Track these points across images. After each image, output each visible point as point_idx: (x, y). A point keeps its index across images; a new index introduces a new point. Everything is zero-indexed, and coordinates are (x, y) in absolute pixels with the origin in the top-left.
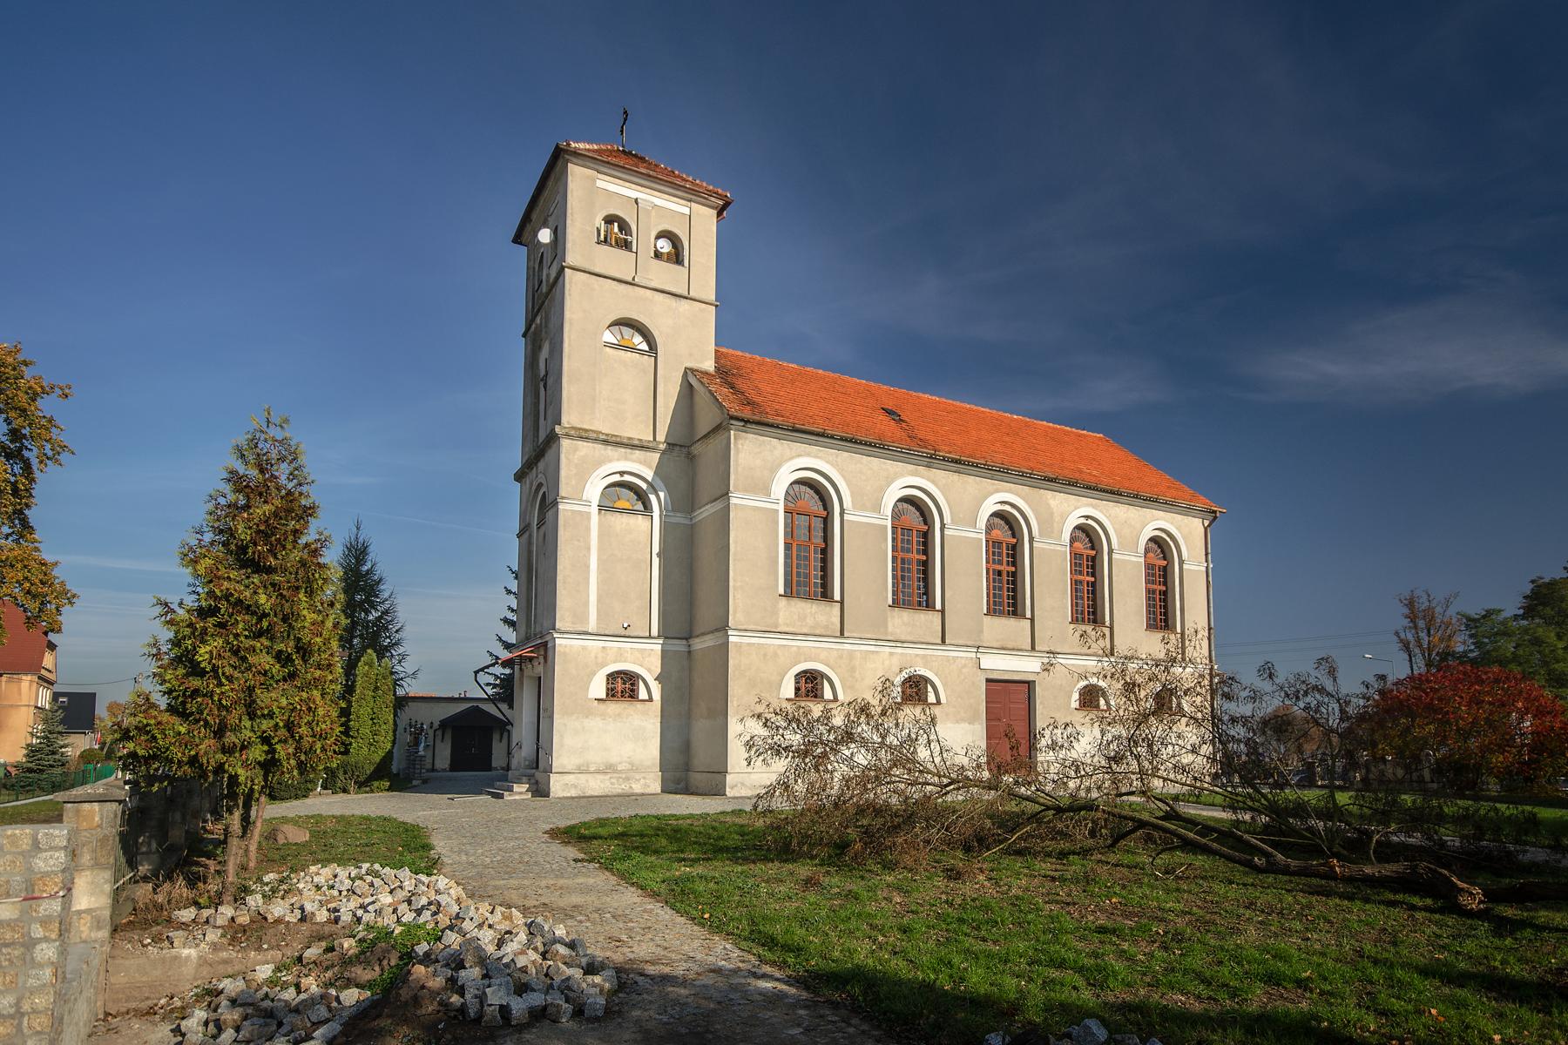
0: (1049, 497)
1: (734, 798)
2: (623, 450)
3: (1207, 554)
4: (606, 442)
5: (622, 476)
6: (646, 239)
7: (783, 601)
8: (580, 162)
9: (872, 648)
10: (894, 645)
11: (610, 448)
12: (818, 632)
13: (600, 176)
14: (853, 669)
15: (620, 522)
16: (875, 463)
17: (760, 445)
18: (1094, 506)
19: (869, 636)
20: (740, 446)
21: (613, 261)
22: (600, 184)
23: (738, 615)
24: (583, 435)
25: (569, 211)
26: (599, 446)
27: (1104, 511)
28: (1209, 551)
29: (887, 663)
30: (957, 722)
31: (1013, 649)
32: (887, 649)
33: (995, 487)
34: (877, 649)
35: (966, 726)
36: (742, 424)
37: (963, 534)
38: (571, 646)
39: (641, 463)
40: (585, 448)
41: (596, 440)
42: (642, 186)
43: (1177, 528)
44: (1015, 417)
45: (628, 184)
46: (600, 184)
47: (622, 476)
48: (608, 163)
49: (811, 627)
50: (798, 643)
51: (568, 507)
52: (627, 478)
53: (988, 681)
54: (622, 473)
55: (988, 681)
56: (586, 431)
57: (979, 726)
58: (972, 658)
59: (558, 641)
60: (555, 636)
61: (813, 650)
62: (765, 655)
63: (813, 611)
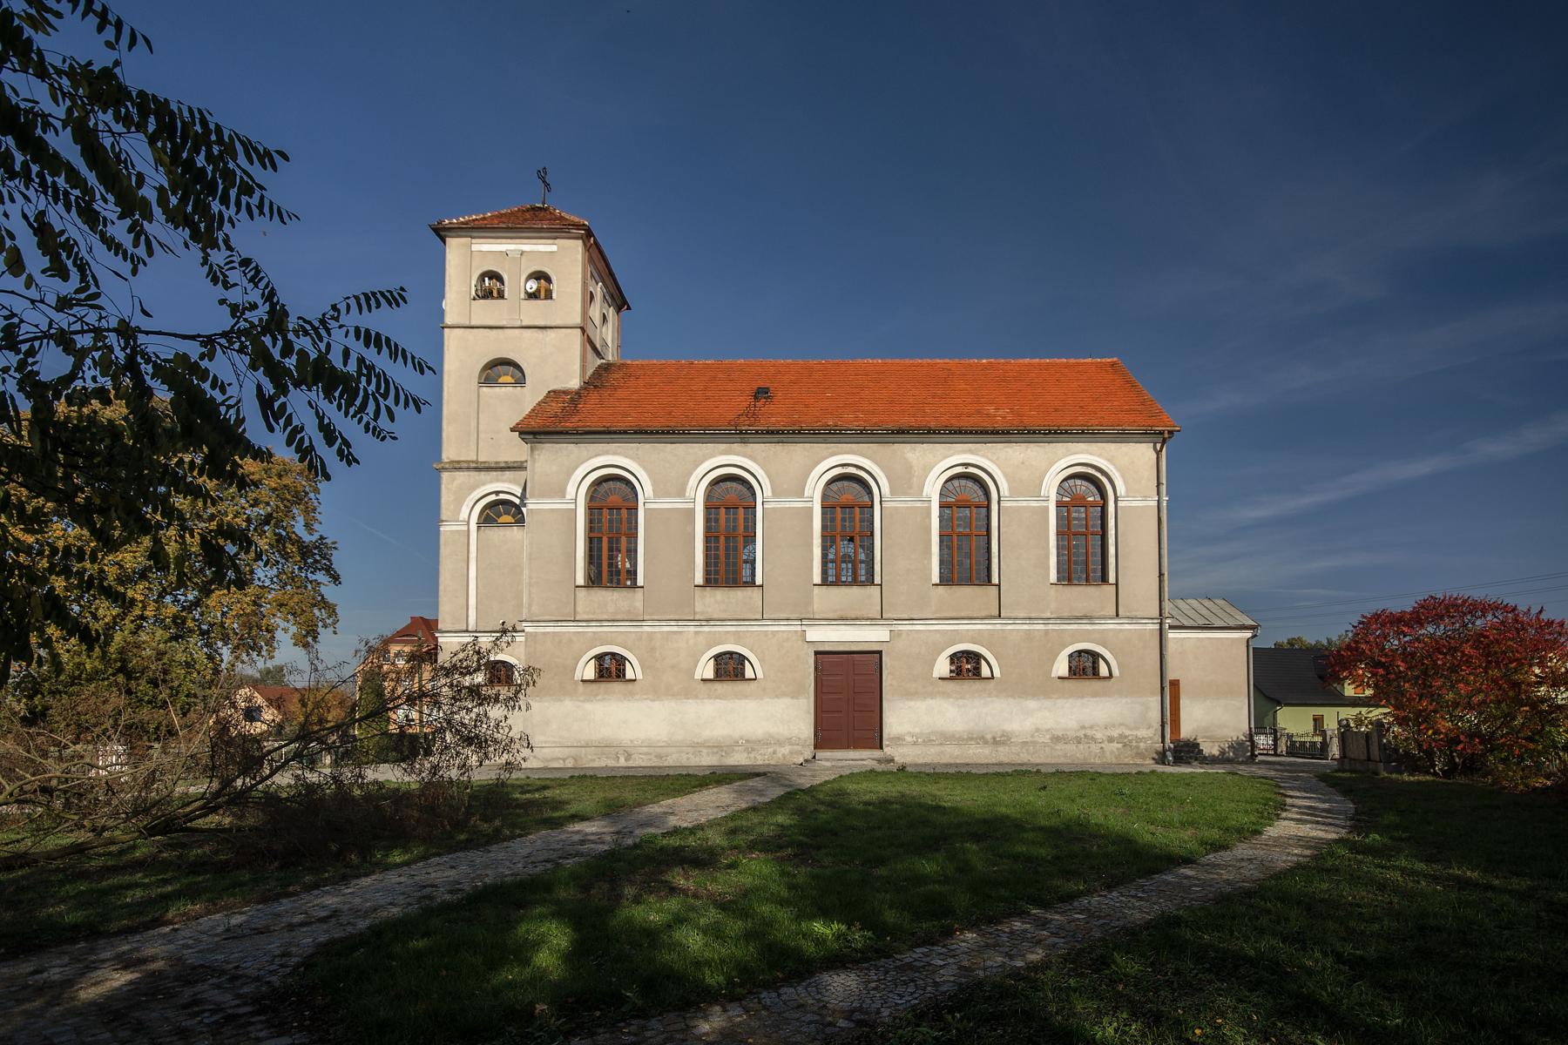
0: (906, 451)
1: (526, 769)
2: (495, 473)
3: (1159, 484)
4: (477, 469)
5: (497, 495)
6: (517, 284)
7: (582, 593)
8: (454, 234)
9: (675, 629)
10: (868, 623)
11: (483, 473)
12: (619, 617)
13: (474, 241)
14: (653, 649)
15: (496, 534)
16: (680, 449)
17: (557, 452)
18: (971, 452)
19: (668, 617)
20: (537, 457)
21: (487, 311)
22: (475, 248)
23: (533, 608)
24: (457, 466)
25: (447, 278)
26: (473, 474)
27: (989, 455)
28: (1164, 481)
29: (691, 642)
30: (777, 697)
31: (857, 619)
32: (692, 629)
33: (830, 451)
34: (681, 629)
35: (787, 701)
36: (531, 436)
37: (787, 505)
38: (451, 642)
39: (510, 482)
40: (461, 477)
41: (468, 469)
42: (511, 238)
43: (1108, 460)
44: (1048, 361)
45: (499, 241)
46: (475, 248)
47: (497, 495)
48: (473, 228)
49: (611, 613)
50: (594, 629)
51: (448, 528)
52: (502, 496)
53: (817, 653)
54: (497, 493)
55: (817, 653)
56: (459, 462)
57: (805, 701)
58: (796, 632)
59: (440, 640)
60: (437, 635)
61: (609, 635)
62: (560, 642)
63: (615, 598)
